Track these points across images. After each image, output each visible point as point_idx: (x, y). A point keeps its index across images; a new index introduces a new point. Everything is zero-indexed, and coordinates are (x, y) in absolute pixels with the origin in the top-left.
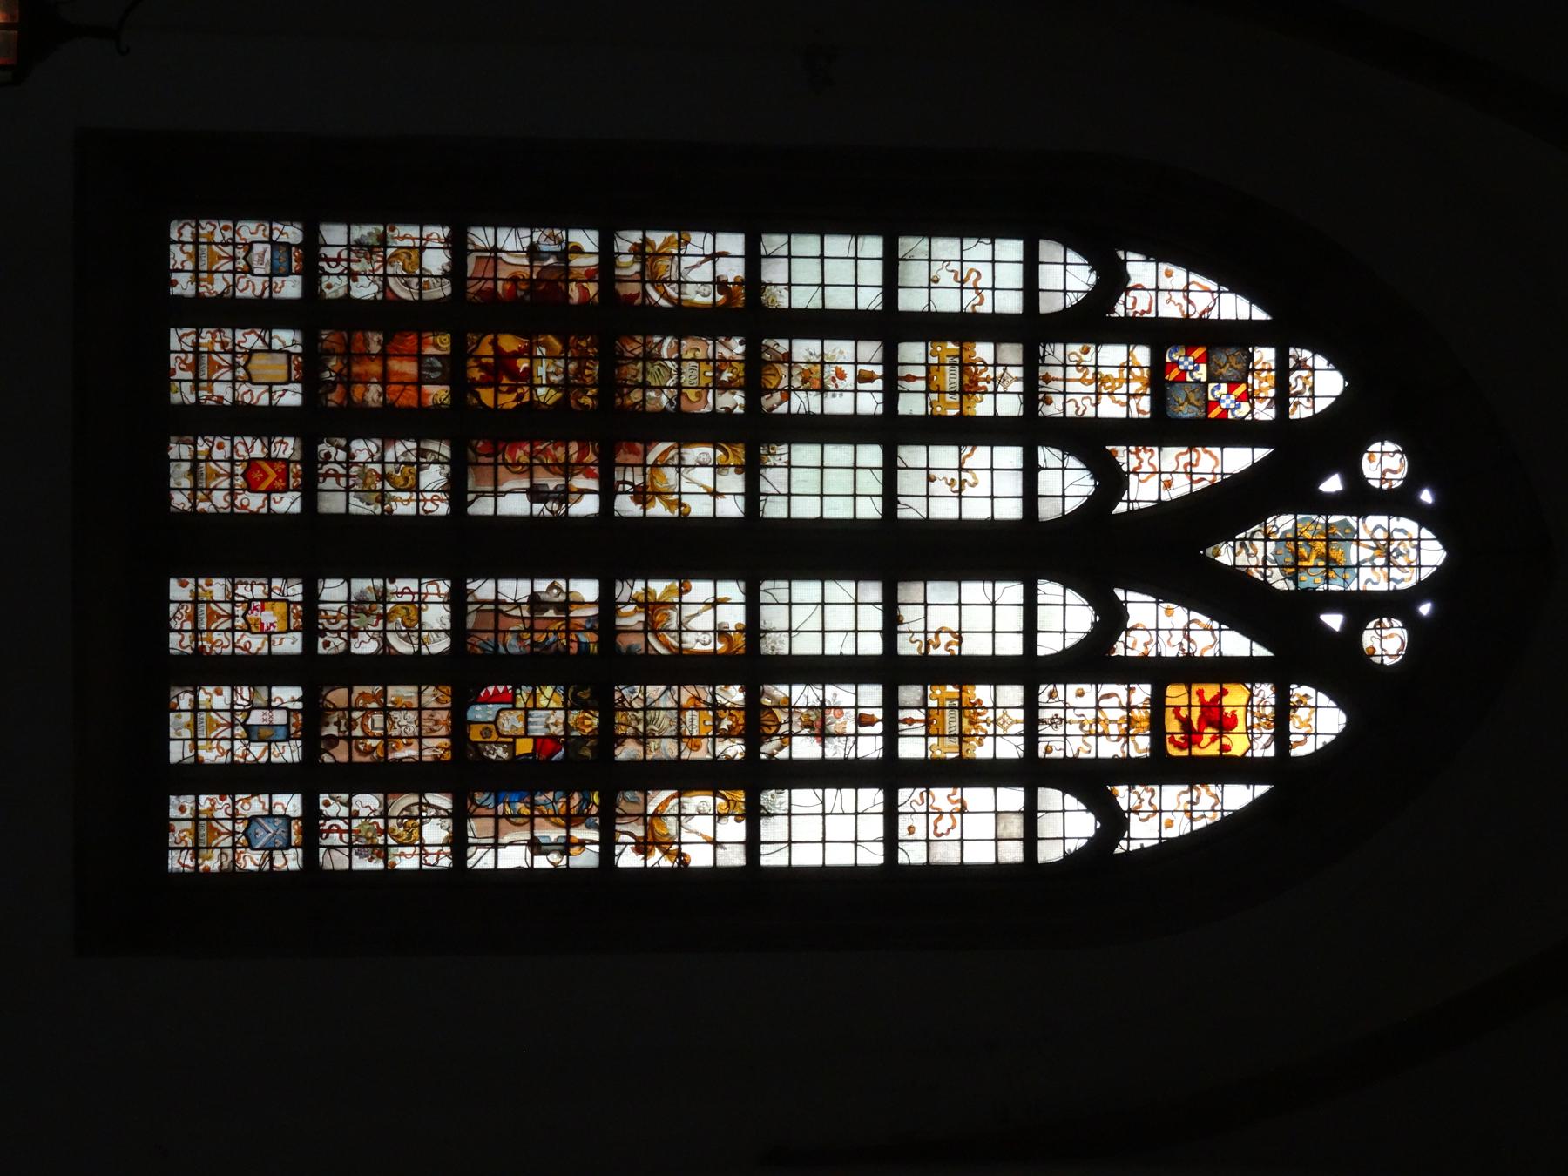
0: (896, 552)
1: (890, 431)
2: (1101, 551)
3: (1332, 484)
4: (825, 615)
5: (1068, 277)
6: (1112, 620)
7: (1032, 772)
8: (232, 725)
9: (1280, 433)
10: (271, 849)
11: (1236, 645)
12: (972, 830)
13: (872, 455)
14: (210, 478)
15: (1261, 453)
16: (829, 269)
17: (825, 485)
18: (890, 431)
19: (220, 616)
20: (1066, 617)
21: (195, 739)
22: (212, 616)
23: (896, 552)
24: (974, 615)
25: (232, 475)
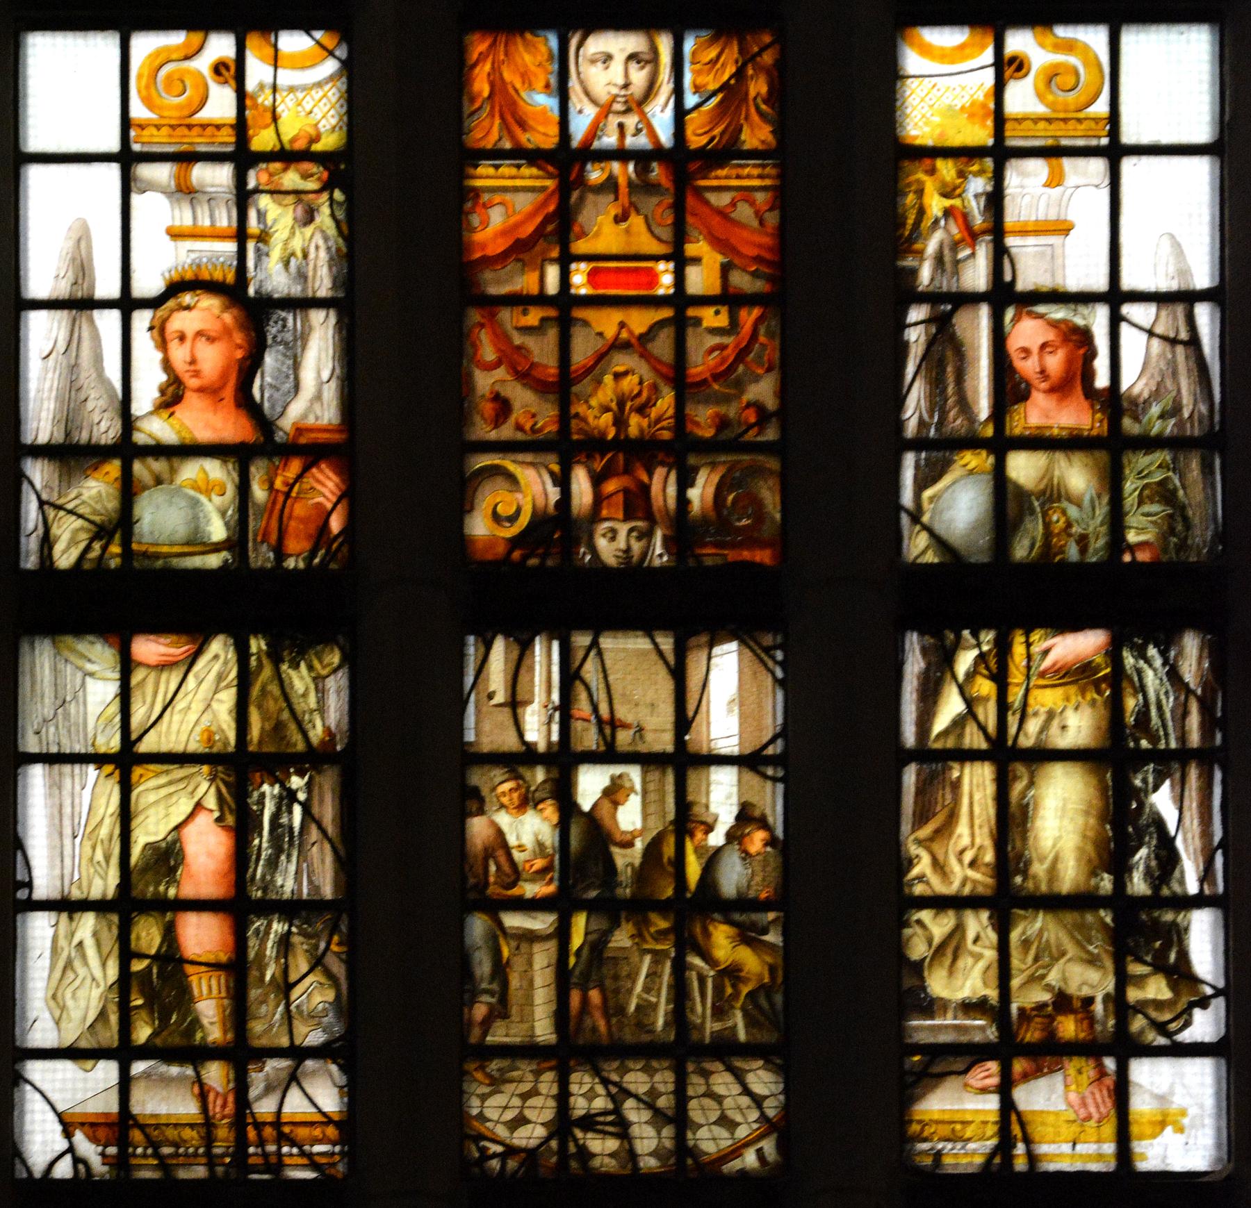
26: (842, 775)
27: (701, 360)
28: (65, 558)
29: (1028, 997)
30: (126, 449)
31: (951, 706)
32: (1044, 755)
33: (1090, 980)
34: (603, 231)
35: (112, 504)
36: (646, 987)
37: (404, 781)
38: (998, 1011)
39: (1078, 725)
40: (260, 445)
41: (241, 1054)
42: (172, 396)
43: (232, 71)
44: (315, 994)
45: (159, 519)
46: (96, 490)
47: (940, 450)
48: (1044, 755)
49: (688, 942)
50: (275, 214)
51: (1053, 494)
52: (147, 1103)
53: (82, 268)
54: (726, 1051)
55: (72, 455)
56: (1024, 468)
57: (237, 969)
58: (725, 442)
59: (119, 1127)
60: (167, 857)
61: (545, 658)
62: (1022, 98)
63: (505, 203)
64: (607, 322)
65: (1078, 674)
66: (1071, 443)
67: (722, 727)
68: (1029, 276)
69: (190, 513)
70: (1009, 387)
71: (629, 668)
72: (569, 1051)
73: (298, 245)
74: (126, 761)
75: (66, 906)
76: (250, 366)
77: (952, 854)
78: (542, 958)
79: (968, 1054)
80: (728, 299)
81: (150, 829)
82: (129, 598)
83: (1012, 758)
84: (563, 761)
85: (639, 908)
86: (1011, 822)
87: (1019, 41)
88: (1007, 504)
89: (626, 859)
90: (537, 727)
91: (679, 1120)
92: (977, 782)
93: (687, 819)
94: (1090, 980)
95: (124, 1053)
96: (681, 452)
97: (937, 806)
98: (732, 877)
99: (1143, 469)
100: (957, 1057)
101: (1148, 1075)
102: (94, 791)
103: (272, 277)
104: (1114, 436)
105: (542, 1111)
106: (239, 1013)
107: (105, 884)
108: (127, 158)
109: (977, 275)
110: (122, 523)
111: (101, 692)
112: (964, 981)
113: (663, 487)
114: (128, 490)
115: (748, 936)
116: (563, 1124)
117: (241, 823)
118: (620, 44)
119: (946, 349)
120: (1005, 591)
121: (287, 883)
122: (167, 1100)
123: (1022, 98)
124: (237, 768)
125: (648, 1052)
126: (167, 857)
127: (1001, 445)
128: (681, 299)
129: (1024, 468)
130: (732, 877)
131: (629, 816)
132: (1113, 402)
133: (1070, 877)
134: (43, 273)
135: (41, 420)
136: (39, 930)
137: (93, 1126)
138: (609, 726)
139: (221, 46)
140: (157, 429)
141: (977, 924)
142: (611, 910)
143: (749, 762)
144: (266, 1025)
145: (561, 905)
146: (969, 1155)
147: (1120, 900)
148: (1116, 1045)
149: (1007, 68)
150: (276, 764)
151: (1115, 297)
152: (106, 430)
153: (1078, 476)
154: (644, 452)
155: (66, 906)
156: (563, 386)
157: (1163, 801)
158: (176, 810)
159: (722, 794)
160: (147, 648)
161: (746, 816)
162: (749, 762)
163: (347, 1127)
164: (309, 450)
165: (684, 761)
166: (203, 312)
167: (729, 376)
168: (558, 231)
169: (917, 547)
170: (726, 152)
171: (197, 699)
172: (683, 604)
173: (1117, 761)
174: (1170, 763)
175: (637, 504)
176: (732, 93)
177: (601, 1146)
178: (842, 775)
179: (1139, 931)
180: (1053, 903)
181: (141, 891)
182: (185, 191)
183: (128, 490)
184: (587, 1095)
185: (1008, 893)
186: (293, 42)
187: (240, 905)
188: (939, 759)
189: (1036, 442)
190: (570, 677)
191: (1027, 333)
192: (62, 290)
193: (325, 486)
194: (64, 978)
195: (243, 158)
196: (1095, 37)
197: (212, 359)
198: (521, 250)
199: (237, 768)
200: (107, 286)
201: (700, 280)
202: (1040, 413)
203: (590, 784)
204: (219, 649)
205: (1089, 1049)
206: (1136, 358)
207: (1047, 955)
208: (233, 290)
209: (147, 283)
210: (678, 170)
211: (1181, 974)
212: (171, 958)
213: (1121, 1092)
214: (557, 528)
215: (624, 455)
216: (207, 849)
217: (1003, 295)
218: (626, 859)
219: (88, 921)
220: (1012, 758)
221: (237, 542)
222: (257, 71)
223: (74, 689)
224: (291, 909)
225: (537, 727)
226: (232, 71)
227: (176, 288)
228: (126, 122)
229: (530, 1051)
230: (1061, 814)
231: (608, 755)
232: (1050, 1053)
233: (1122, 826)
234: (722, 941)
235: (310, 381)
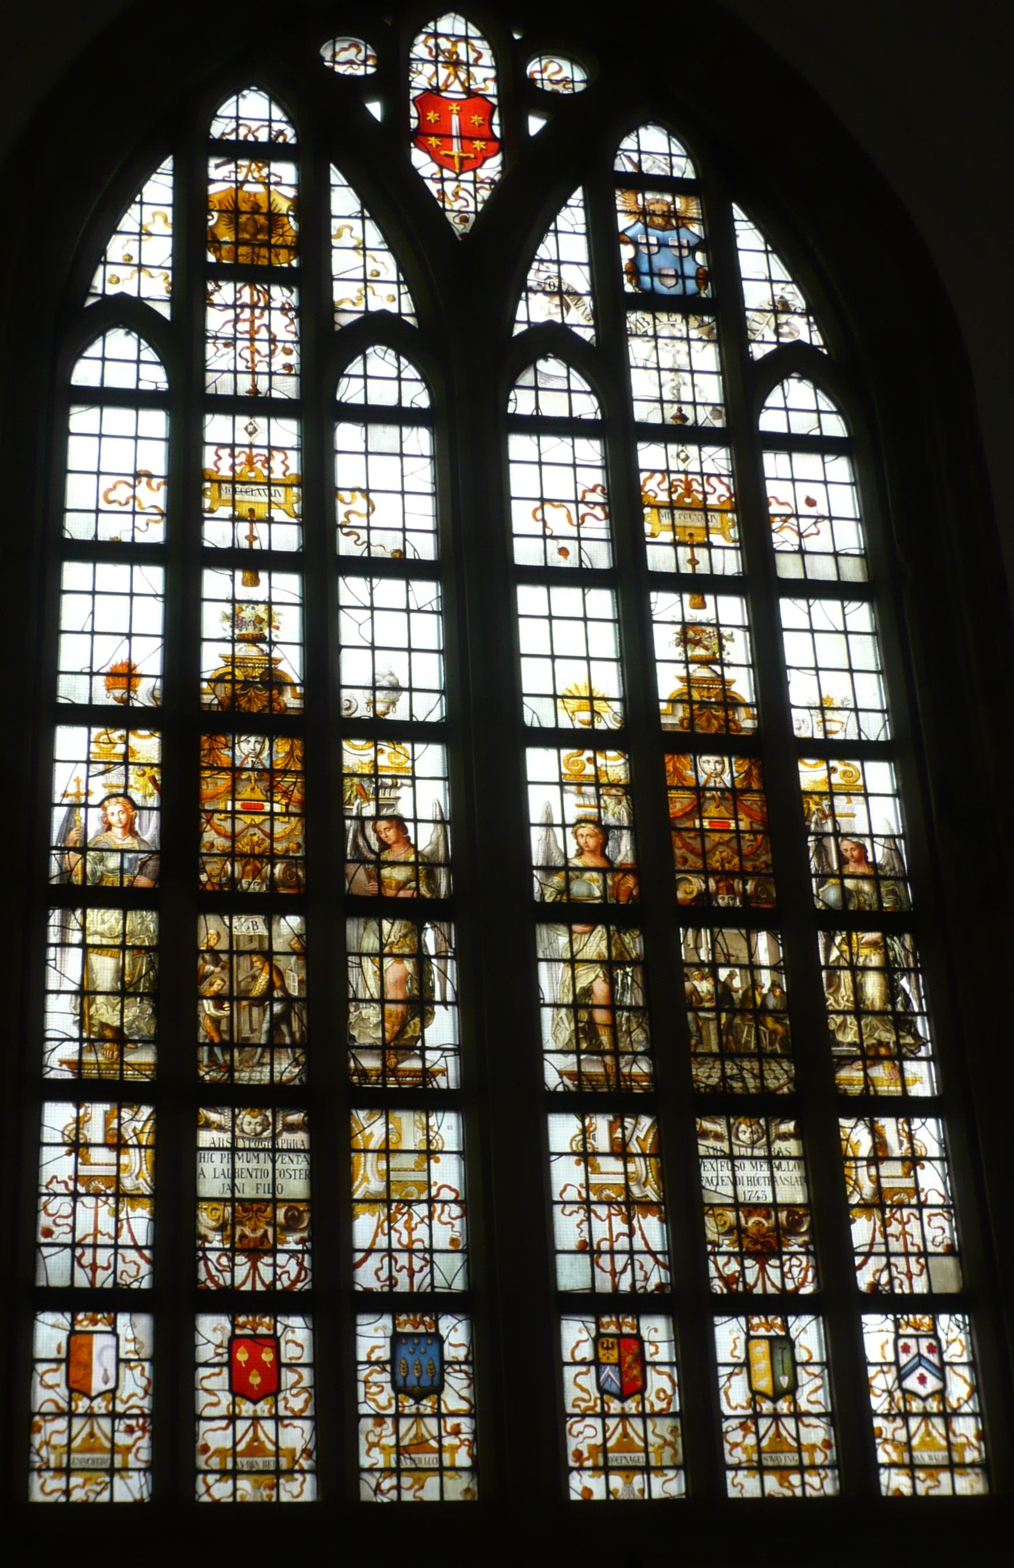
0: (476, 572)
1: (320, 565)
2: (466, 342)
3: (375, 109)
4: (564, 653)
5: (116, 358)
6: (553, 339)
7: (742, 436)
8: (776, 1416)
9: (312, 158)
10: (944, 1364)
11: (572, 217)
12: (820, 507)
13: (351, 589)
14: (422, 1448)
15: (336, 177)
16: (105, 627)
17: (394, 645)
18: (320, 565)
19: (625, 1434)
20: (553, 388)
21: (801, 1469)
22: (625, 1444)
23: (476, 572)
24: (551, 489)
25: (418, 1416)
26: (802, 971)
27: (746, 847)
28: (549, 899)
29: (869, 1042)
30: (566, 868)
31: (835, 953)
32: (865, 969)
33: (889, 1037)
34: (712, 810)
35: (563, 884)
36: (747, 1035)
37: (662, 971)
38: (860, 1046)
39: (875, 960)
40: (608, 868)
41: (617, 1053)
42: (580, 853)
43: (593, 761)
44: (639, 1035)
45: (578, 889)
46: (557, 880)
47: (823, 878)
48: (865, 969)
49: (759, 1022)
50: (608, 801)
51: (859, 892)
52: (587, 1068)
53: (549, 815)
54: (774, 1056)
55: (549, 869)
56: (849, 883)
57: (613, 1027)
58: (755, 874)
59: (578, 1075)
60: (588, 991)
61: (705, 935)
62: (836, 779)
63: (679, 802)
64: (716, 837)
65: (873, 944)
66: (863, 877)
67: (764, 957)
68: (844, 829)
69: (589, 887)
70: (842, 861)
71: (732, 939)
72: (724, 1055)
73: (616, 812)
74: (573, 962)
75: (556, 1006)
76: (604, 845)
77: (842, 997)
78: (712, 1026)
79: (850, 1059)
80: (752, 831)
81: (582, 983)
82: (570, 913)
83: (857, 970)
84: (713, 967)
85: (742, 1011)
86: (858, 989)
87: (833, 763)
88: (846, 894)
89: (738, 996)
90: (704, 955)
91: (761, 1077)
92: (846, 976)
93: (755, 985)
94: (889, 1037)
95: (578, 1052)
96: (743, 875)
97: (834, 984)
98: (771, 1003)
99: (885, 887)
100: (848, 1060)
101: (910, 1066)
102: (562, 971)
103: (609, 819)
104: (876, 874)
105: (716, 1074)
106: (615, 1040)
107: (569, 999)
108: (561, 784)
109: (829, 827)
110: (566, 890)
111: (563, 940)
112: (849, 1036)
113: (738, 885)
114: (568, 880)
115: (777, 1020)
116: (724, 1077)
117: (611, 982)
118: (713, 759)
119: (822, 850)
120: (847, 918)
121: (628, 1000)
122: (593, 1067)
123: (836, 779)
124: (609, 965)
125: (750, 1056)
126: (588, 991)
127: (842, 877)
128: (738, 831)
129: (849, 883)
130: (771, 1003)
131: (737, 983)
132: (874, 865)
133: (878, 1005)
134: (536, 815)
135: (537, 857)
136: (547, 1013)
137: (570, 1075)
138: (728, 956)
139: (589, 753)
140: (576, 862)
141: (850, 1019)
142: (733, 1012)
143: (773, 968)
144: (624, 1044)
145: (717, 1010)
146: (856, 1089)
147: (894, 1012)
148: (898, 1057)
149: (831, 770)
150: (622, 964)
151: (871, 836)
152: (559, 862)
153: (866, 887)
154: (730, 875)
155: (556, 1006)
156: (704, 854)
157: (904, 982)
158: (588, 976)
159: (766, 978)
160: (577, 928)
161: (775, 985)
162: (773, 968)
163: (651, 1077)
164: (624, 870)
165: (752, 967)
166: (587, 829)
167: (754, 854)
168: (697, 810)
169: (819, 905)
170: (748, 790)
171: (594, 943)
172: (749, 919)
173: (889, 971)
174: (906, 971)
175: (730, 890)
176: (748, 773)
177: (737, 1085)
178: (802, 971)
179: (902, 1022)
180: (873, 1013)
181: (579, 1003)
182: (580, 794)
183: (568, 880)
184: (731, 1069)
185: (859, 1009)
186: (611, 754)
187: (613, 1006)
188: (833, 969)
189: (852, 876)
190: (714, 941)
191: (846, 845)
192: (544, 821)
193: (630, 882)
194: (554, 1029)
195: (598, 785)
196: (857, 764)
197: (592, 842)
198: (687, 815)
199: (609, 965)
200: (558, 820)
201: (743, 825)
202: (851, 868)
203: (723, 973)
204: (600, 930)
205: (890, 1058)
206: (879, 853)
207: (874, 1029)
208: (597, 822)
209: (570, 819)
210: (733, 795)
211: (916, 1035)
212: (591, 1022)
213: (901, 1071)
214: (705, 896)
215: (725, 876)
216: (601, 989)
217: (837, 834)
218: (738, 996)
219: (563, 1011)
220: (857, 970)
221: (604, 896)
222: (600, 761)
223: (554, 940)
224: (629, 1008)
225: (704, 955)
226: (593, 761)
227: (579, 821)
228: (561, 774)
229: (711, 1054)
230: (873, 987)
231: (728, 964)
232: (878, 1059)
233: (892, 991)
234: (770, 1022)
235: (623, 850)
